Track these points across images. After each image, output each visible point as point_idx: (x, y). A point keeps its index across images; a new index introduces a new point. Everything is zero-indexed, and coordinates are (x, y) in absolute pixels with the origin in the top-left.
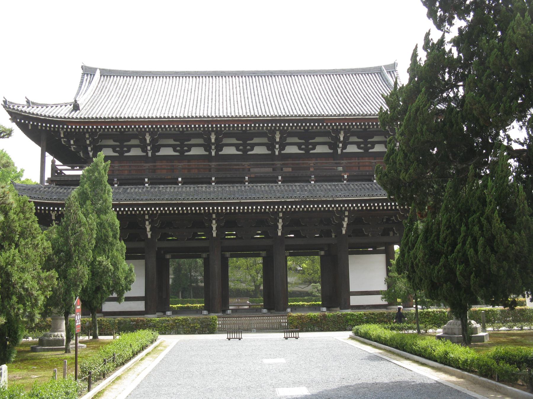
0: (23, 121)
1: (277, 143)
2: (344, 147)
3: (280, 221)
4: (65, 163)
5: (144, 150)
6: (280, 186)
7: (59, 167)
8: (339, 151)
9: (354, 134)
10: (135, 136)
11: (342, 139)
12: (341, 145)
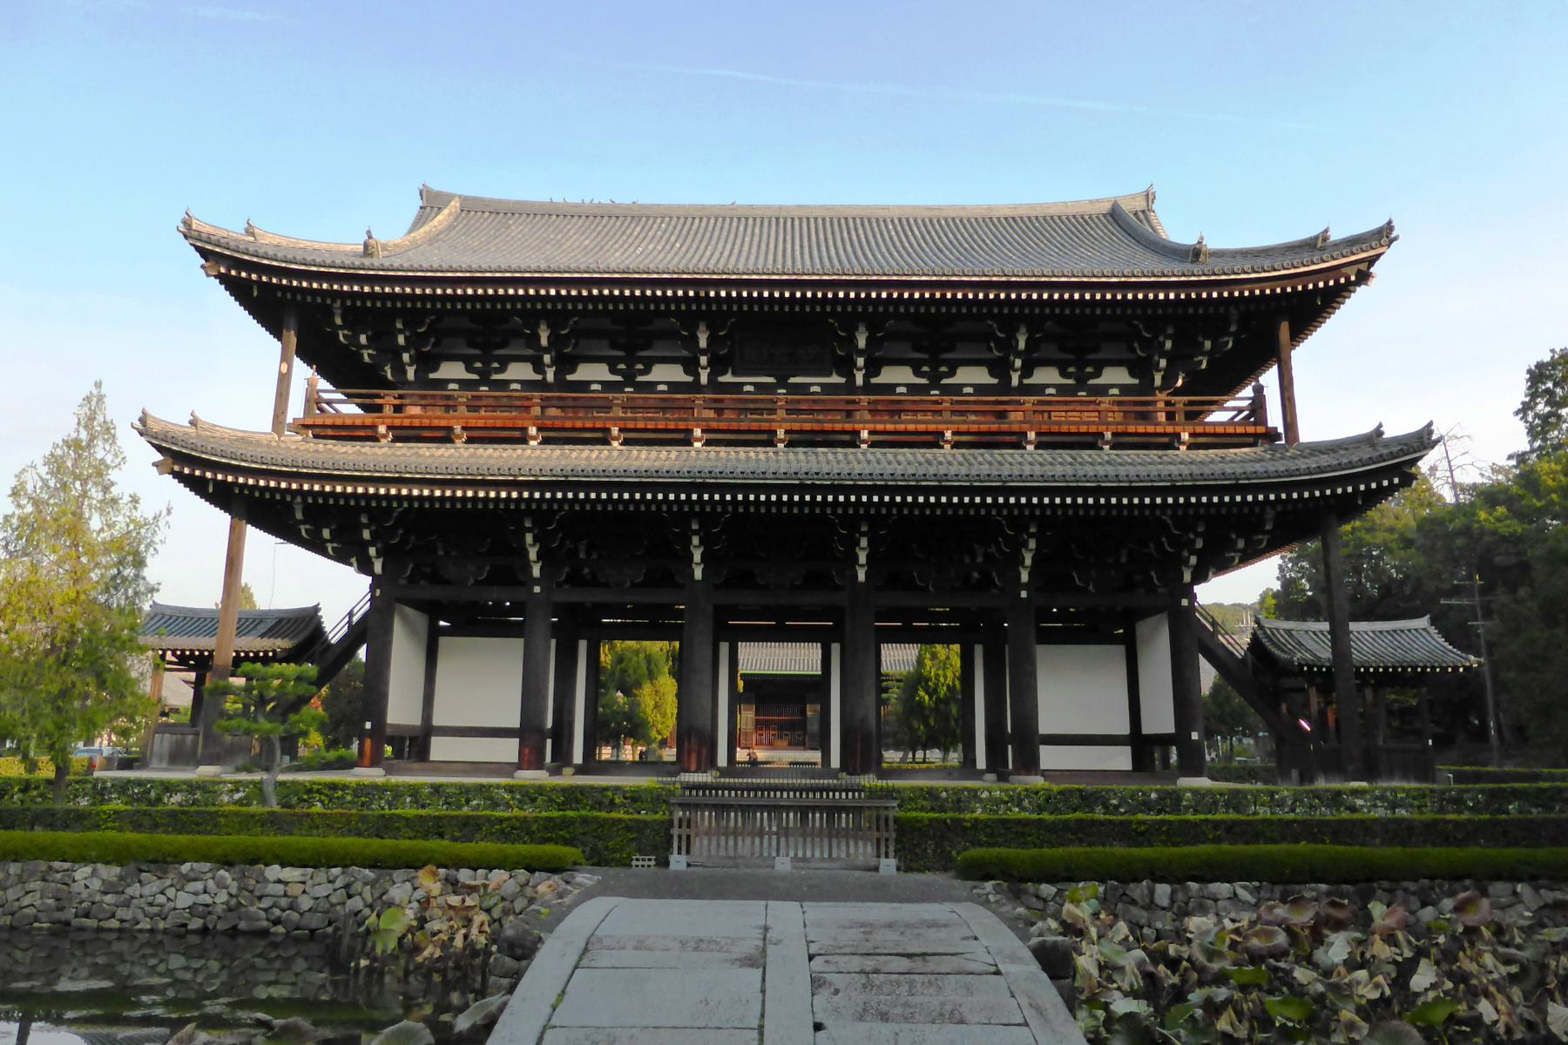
1: (860, 353)
2: (1027, 371)
3: (864, 542)
4: (338, 383)
5: (539, 367)
7: (325, 396)
8: (1015, 381)
10: (517, 334)
12: (1018, 363)
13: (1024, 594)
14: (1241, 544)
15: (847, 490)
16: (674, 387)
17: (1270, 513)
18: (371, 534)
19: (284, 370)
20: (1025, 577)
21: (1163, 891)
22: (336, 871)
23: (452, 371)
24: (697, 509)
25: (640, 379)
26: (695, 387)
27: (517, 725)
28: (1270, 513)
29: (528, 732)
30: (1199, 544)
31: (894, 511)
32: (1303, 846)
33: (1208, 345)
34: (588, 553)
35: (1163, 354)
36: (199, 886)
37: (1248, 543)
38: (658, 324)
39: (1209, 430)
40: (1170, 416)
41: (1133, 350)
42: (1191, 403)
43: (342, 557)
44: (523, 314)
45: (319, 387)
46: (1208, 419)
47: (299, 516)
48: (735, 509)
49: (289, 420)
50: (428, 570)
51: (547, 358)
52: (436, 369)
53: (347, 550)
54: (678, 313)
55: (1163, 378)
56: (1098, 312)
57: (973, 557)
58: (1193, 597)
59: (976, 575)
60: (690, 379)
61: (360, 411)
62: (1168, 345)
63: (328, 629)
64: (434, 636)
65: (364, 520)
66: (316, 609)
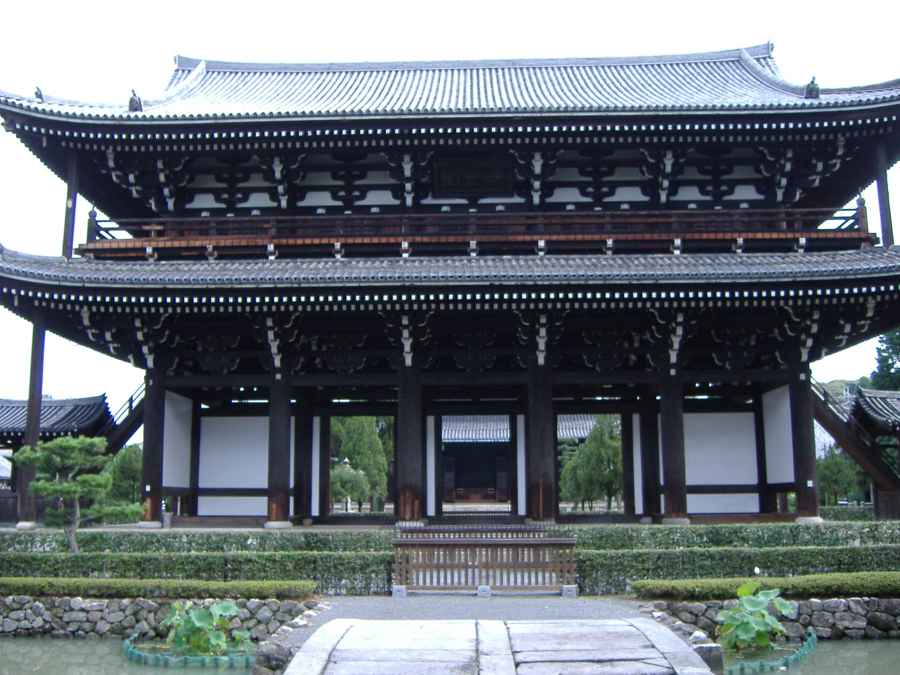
0: (26, 128)
2: (673, 191)
3: (543, 332)
5: (274, 196)
6: (541, 260)
7: (103, 225)
8: (663, 198)
9: (690, 162)
10: (257, 170)
11: (669, 169)
12: (666, 183)
13: (673, 372)
14: (848, 328)
15: (528, 289)
16: (384, 208)
17: (871, 304)
18: (144, 335)
19: (70, 205)
20: (673, 358)
22: (126, 601)
23: (205, 202)
24: (406, 307)
26: (402, 208)
27: (265, 485)
28: (871, 304)
29: (275, 492)
30: (815, 329)
31: (568, 305)
33: (820, 167)
34: (319, 346)
35: (784, 175)
36: (21, 614)
37: (855, 328)
38: (371, 158)
39: (821, 235)
40: (790, 225)
41: (758, 171)
42: (807, 214)
43: (121, 355)
44: (260, 152)
45: (97, 219)
46: (820, 227)
47: (86, 322)
48: (438, 307)
49: (75, 246)
50: (191, 363)
51: (281, 189)
52: (191, 200)
53: (125, 350)
54: (386, 149)
55: (785, 194)
56: (731, 139)
57: (631, 343)
58: (808, 372)
59: (633, 357)
60: (397, 202)
61: (130, 237)
62: (788, 167)
63: (113, 414)
65: (138, 323)
66: (104, 397)
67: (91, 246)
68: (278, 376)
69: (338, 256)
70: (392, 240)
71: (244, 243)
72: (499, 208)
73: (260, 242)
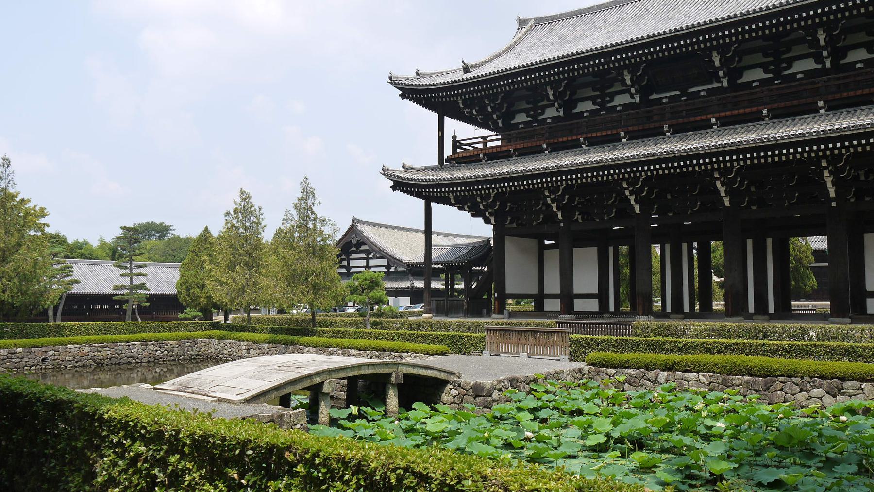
16: (626, 106)
20: (832, 194)
21: (663, 375)
23: (521, 118)
25: (609, 105)
32: (743, 357)
49: (445, 157)
52: (513, 118)
64: (542, 248)
67: (457, 156)
68: (562, 225)
69: (584, 146)
70: (615, 132)
71: (530, 145)
72: (702, 93)
73: (538, 143)
